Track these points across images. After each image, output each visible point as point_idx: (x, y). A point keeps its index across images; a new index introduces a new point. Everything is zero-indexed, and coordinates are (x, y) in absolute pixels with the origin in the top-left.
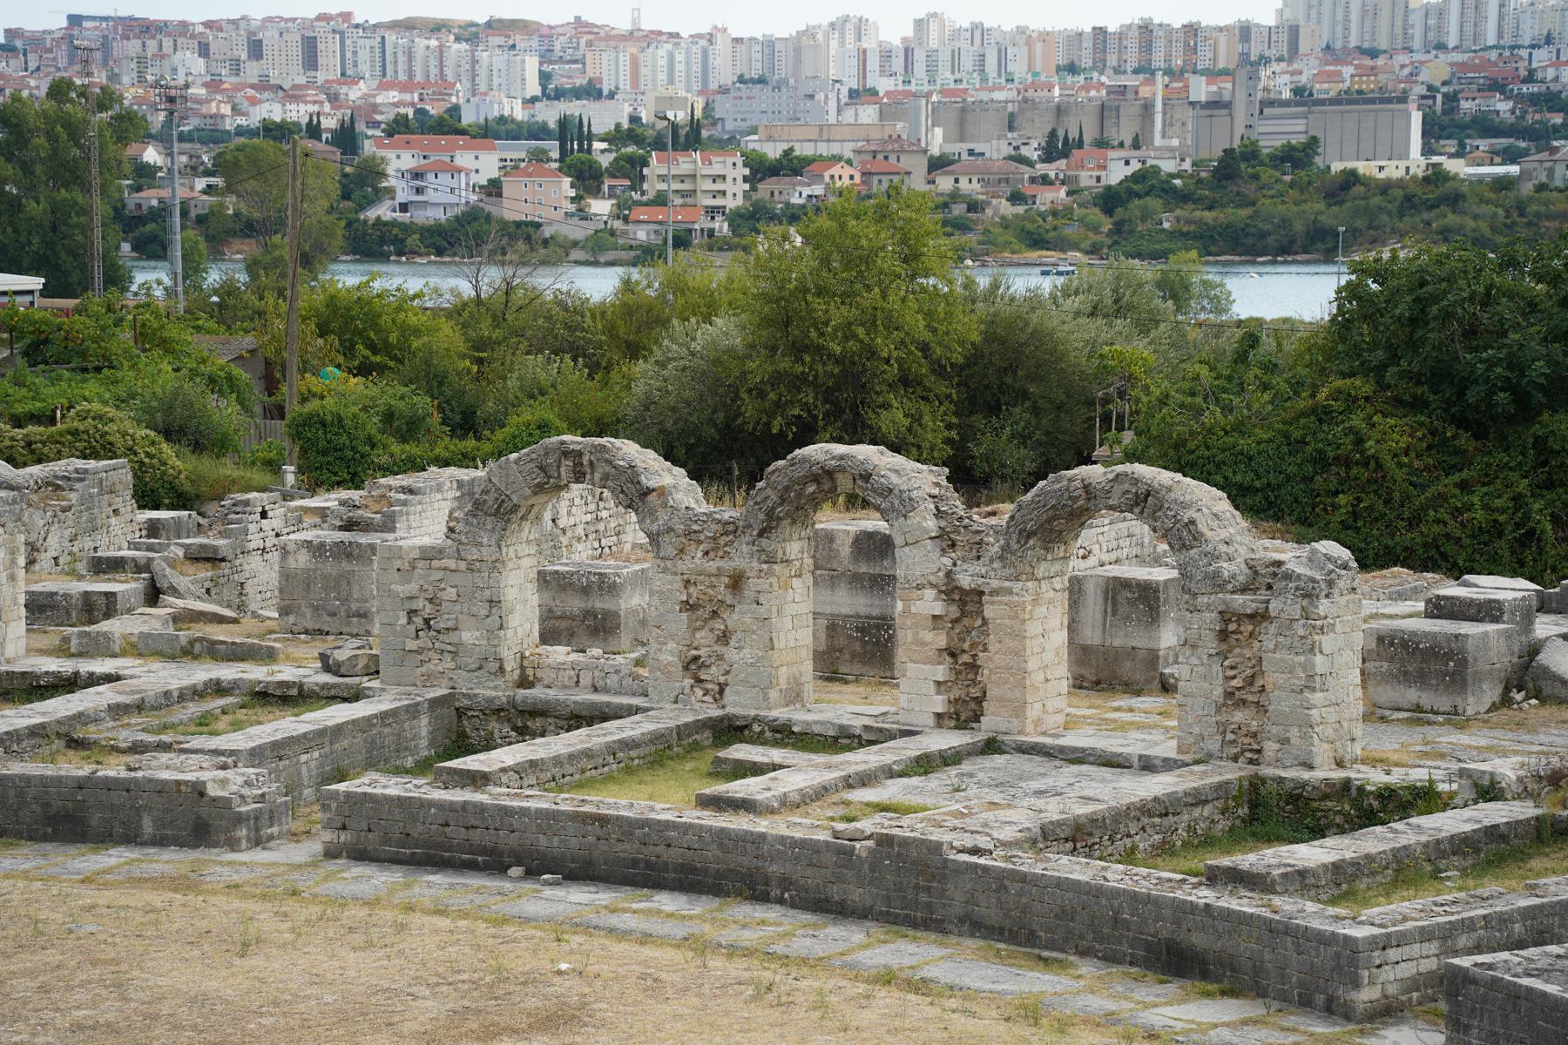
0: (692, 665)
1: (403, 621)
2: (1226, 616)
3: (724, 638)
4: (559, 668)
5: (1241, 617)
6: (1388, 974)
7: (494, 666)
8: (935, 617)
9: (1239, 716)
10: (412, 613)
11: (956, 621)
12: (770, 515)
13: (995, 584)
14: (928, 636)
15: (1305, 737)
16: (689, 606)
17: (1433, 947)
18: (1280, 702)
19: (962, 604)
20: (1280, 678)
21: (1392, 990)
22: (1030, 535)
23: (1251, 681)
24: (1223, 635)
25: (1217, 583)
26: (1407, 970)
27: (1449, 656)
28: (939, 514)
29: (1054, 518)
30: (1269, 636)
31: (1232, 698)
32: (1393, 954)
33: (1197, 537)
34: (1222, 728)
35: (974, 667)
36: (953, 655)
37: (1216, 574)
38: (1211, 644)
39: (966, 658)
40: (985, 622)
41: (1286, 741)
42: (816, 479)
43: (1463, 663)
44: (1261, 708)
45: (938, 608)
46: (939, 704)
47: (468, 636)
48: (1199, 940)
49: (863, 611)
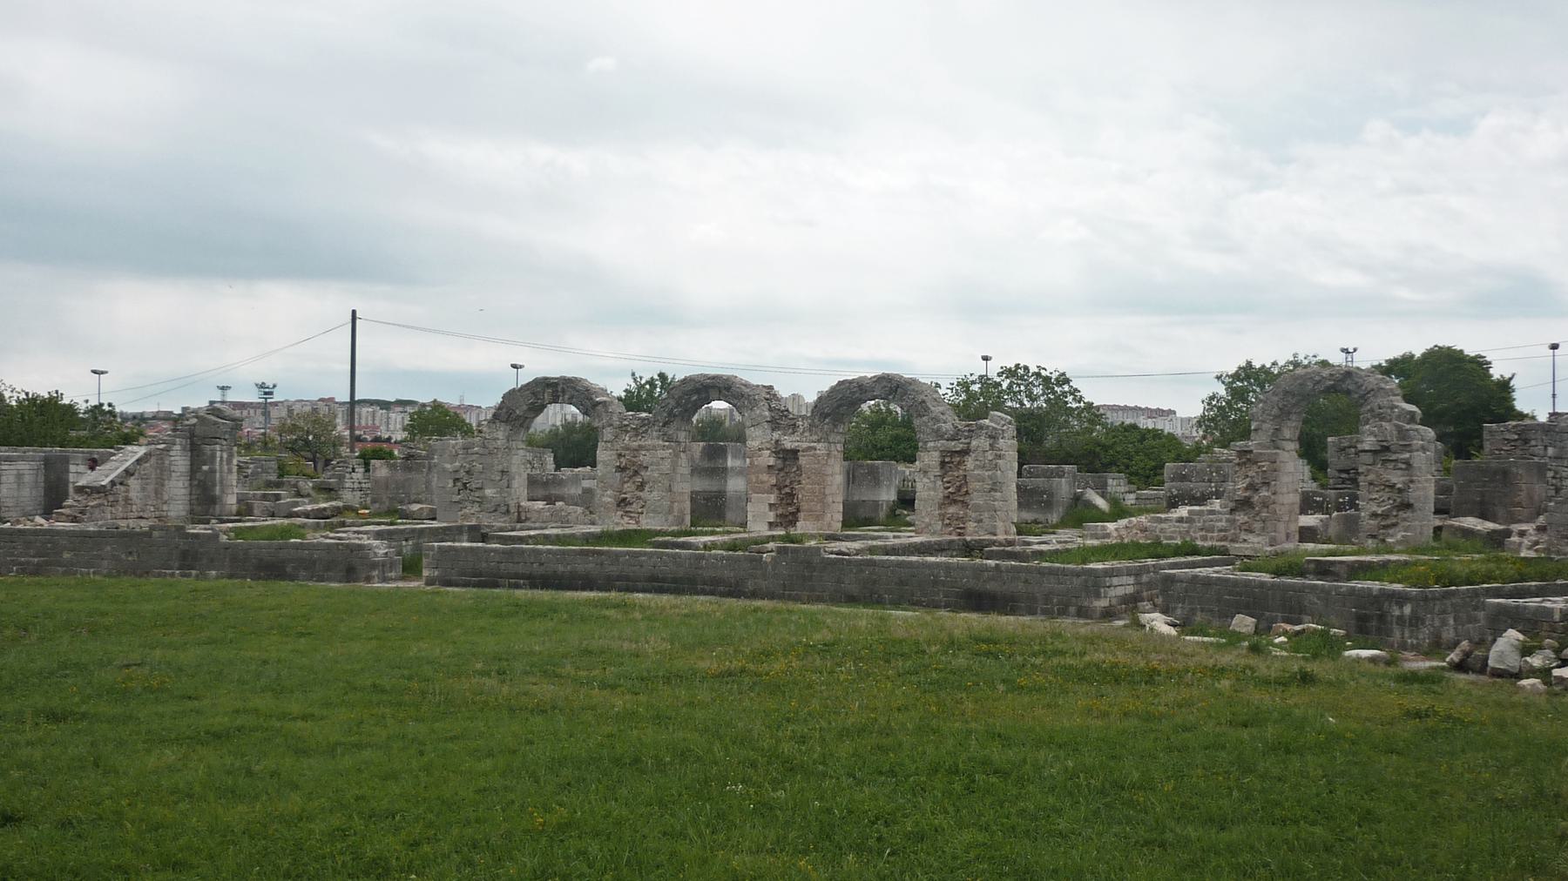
0: (622, 503)
1: (451, 484)
2: (945, 453)
3: (641, 487)
4: (539, 511)
5: (953, 453)
6: (1112, 592)
7: (504, 509)
8: (769, 467)
9: (952, 510)
10: (456, 480)
11: (780, 470)
12: (670, 413)
13: (805, 445)
14: (765, 477)
15: (992, 518)
16: (621, 469)
17: (1131, 580)
18: (977, 499)
19: (785, 459)
20: (977, 485)
21: (1114, 602)
22: (827, 415)
23: (959, 489)
24: (943, 464)
25: (939, 435)
26: (1120, 591)
27: (1044, 492)
28: (770, 409)
29: (839, 406)
30: (970, 462)
31: (949, 500)
32: (1115, 581)
33: (927, 409)
34: (942, 517)
35: (791, 495)
36: (780, 489)
37: (939, 429)
38: (937, 471)
39: (787, 490)
40: (799, 468)
41: (980, 521)
42: (697, 391)
43: (1051, 495)
44: (965, 504)
45: (772, 461)
46: (771, 517)
47: (489, 492)
48: (991, 586)
49: (708, 488)
